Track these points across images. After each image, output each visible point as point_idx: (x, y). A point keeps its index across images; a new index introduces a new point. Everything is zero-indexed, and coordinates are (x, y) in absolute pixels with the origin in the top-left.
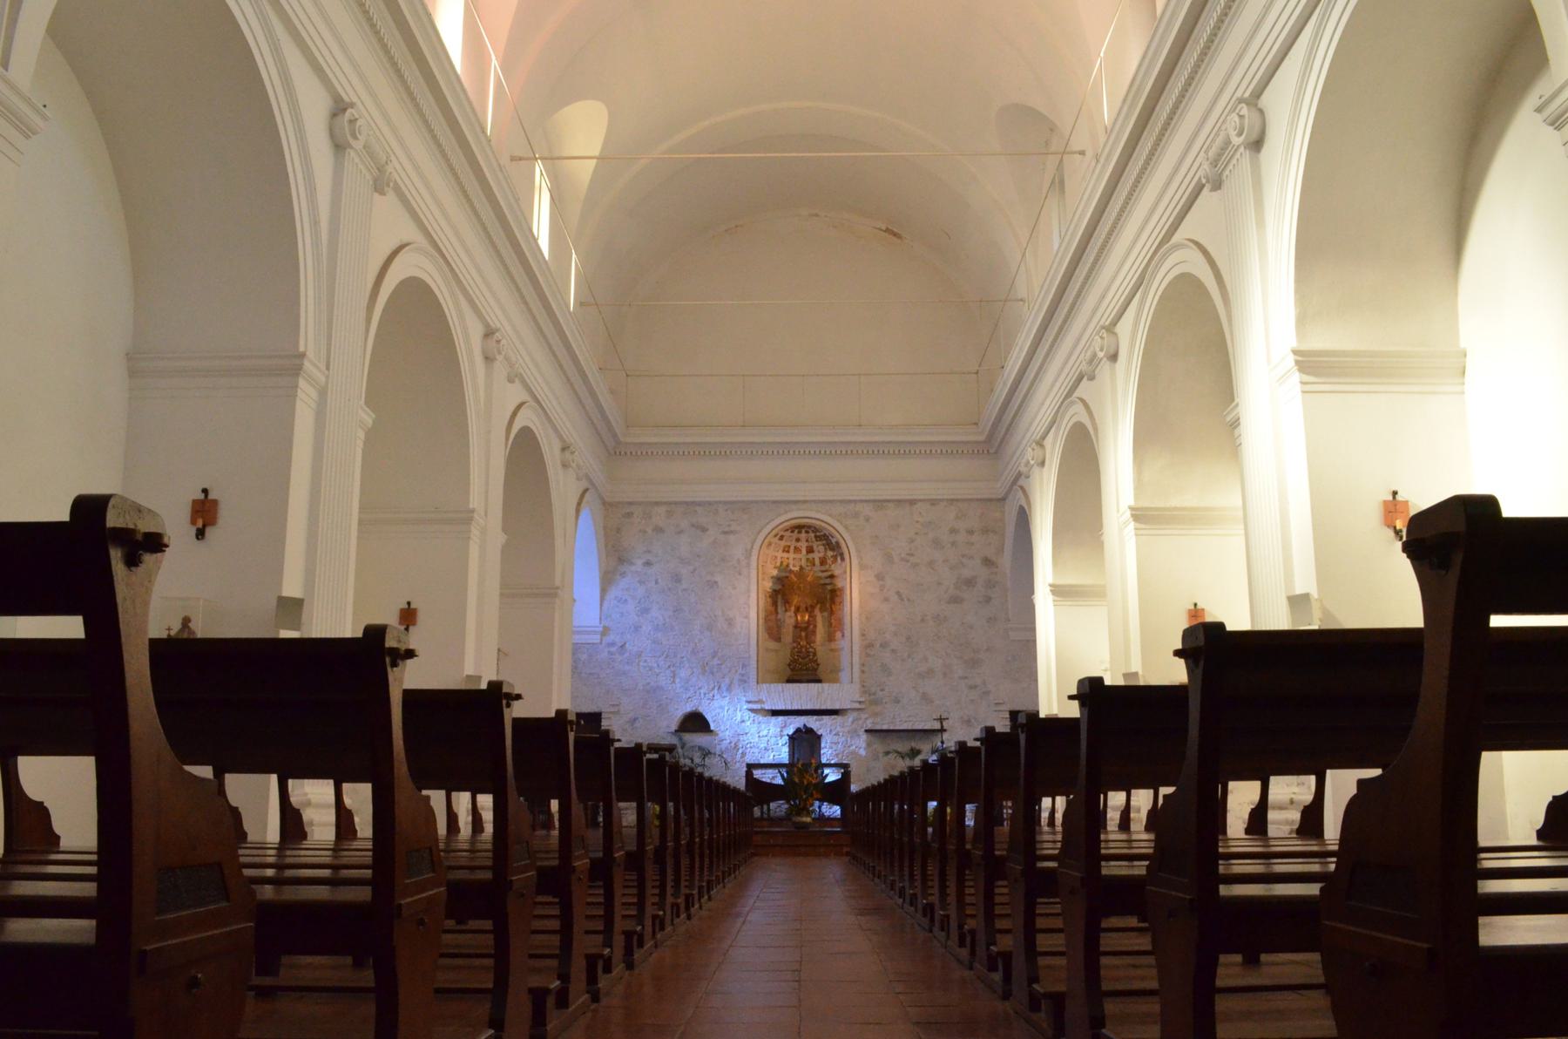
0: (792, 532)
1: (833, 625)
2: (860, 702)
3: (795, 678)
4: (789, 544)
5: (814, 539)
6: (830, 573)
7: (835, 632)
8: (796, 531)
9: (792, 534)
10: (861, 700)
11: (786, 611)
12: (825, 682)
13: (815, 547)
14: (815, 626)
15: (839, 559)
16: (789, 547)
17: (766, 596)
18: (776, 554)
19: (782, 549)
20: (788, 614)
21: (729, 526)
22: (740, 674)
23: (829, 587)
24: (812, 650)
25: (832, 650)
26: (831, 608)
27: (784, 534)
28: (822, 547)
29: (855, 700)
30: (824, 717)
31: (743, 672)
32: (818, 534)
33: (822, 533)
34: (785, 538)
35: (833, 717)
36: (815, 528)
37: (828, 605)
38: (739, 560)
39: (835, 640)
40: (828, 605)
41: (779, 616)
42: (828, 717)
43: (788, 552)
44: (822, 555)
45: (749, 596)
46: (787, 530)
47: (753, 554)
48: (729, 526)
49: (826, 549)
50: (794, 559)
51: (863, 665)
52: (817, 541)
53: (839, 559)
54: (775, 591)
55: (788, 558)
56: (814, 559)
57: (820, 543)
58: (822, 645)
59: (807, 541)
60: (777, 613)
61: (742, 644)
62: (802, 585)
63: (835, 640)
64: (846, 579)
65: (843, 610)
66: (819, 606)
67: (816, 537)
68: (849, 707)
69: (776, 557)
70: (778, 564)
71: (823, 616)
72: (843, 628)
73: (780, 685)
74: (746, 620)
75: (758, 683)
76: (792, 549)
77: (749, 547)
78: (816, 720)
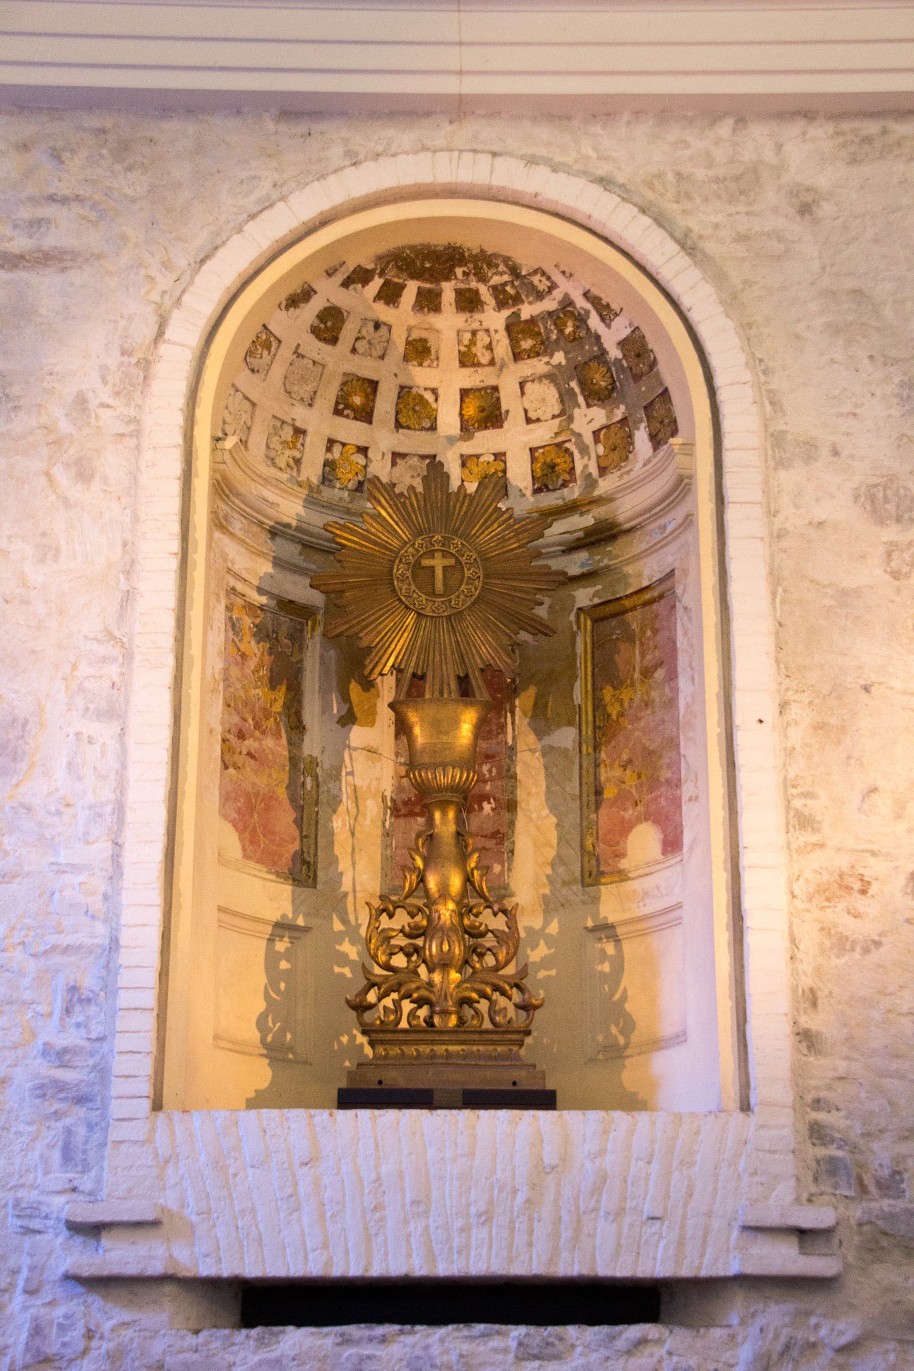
0: (390, 294)
1: (609, 793)
2: (802, 1234)
3: (396, 1079)
4: (366, 368)
5: (503, 347)
6: (587, 520)
7: (626, 828)
8: (412, 288)
9: (383, 312)
10: (808, 1218)
11: (348, 719)
12: (584, 1104)
13: (509, 399)
14: (511, 806)
15: (641, 437)
16: (374, 385)
17: (233, 625)
18: (300, 415)
19: (329, 395)
20: (358, 735)
21: (36, 224)
22: (47, 1051)
23: (584, 596)
24: (499, 923)
25: (606, 930)
26: (598, 704)
27: (343, 298)
28: (550, 393)
29: (773, 1219)
30: (571, 1331)
31: (71, 1038)
32: (527, 311)
33: (550, 304)
34: (348, 333)
35: (634, 1331)
36: (514, 271)
37: (579, 693)
38: (81, 401)
39: (622, 876)
40: (579, 693)
41: (311, 746)
42: (592, 1333)
43: (365, 415)
44: (542, 434)
45: (128, 597)
46: (361, 276)
47: (160, 369)
48: (36, 224)
49: (566, 397)
50: (397, 456)
51: (812, 999)
52: (517, 357)
53: (641, 437)
54: (286, 605)
55: (363, 450)
56: (500, 456)
57: (539, 366)
58: (549, 906)
59: (467, 360)
60: (297, 727)
61: (75, 868)
62: (438, 563)
63: (622, 876)
64: (689, 521)
65: (671, 703)
66: (524, 701)
67: (514, 328)
68: (733, 1269)
69: (299, 432)
70: (312, 471)
71: (547, 751)
72: (676, 803)
73: (297, 1114)
74: (105, 732)
75: (157, 1106)
76: (385, 404)
77: (144, 331)
78: (525, 1354)
